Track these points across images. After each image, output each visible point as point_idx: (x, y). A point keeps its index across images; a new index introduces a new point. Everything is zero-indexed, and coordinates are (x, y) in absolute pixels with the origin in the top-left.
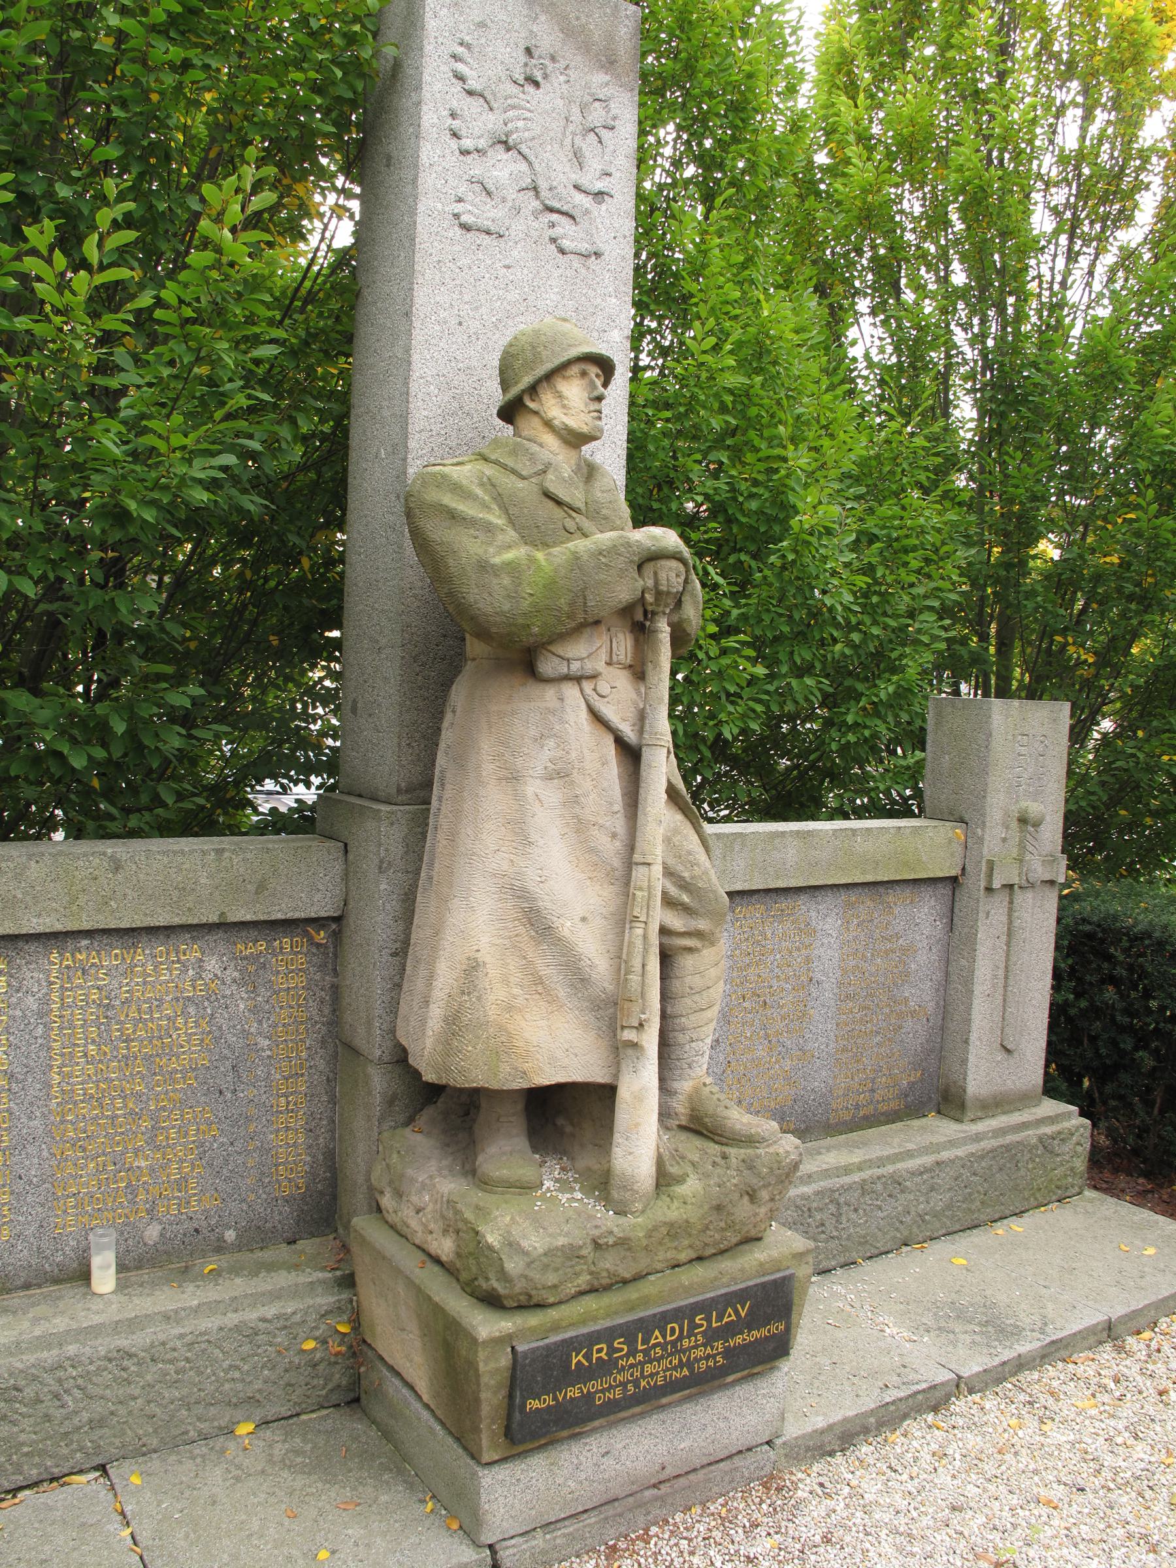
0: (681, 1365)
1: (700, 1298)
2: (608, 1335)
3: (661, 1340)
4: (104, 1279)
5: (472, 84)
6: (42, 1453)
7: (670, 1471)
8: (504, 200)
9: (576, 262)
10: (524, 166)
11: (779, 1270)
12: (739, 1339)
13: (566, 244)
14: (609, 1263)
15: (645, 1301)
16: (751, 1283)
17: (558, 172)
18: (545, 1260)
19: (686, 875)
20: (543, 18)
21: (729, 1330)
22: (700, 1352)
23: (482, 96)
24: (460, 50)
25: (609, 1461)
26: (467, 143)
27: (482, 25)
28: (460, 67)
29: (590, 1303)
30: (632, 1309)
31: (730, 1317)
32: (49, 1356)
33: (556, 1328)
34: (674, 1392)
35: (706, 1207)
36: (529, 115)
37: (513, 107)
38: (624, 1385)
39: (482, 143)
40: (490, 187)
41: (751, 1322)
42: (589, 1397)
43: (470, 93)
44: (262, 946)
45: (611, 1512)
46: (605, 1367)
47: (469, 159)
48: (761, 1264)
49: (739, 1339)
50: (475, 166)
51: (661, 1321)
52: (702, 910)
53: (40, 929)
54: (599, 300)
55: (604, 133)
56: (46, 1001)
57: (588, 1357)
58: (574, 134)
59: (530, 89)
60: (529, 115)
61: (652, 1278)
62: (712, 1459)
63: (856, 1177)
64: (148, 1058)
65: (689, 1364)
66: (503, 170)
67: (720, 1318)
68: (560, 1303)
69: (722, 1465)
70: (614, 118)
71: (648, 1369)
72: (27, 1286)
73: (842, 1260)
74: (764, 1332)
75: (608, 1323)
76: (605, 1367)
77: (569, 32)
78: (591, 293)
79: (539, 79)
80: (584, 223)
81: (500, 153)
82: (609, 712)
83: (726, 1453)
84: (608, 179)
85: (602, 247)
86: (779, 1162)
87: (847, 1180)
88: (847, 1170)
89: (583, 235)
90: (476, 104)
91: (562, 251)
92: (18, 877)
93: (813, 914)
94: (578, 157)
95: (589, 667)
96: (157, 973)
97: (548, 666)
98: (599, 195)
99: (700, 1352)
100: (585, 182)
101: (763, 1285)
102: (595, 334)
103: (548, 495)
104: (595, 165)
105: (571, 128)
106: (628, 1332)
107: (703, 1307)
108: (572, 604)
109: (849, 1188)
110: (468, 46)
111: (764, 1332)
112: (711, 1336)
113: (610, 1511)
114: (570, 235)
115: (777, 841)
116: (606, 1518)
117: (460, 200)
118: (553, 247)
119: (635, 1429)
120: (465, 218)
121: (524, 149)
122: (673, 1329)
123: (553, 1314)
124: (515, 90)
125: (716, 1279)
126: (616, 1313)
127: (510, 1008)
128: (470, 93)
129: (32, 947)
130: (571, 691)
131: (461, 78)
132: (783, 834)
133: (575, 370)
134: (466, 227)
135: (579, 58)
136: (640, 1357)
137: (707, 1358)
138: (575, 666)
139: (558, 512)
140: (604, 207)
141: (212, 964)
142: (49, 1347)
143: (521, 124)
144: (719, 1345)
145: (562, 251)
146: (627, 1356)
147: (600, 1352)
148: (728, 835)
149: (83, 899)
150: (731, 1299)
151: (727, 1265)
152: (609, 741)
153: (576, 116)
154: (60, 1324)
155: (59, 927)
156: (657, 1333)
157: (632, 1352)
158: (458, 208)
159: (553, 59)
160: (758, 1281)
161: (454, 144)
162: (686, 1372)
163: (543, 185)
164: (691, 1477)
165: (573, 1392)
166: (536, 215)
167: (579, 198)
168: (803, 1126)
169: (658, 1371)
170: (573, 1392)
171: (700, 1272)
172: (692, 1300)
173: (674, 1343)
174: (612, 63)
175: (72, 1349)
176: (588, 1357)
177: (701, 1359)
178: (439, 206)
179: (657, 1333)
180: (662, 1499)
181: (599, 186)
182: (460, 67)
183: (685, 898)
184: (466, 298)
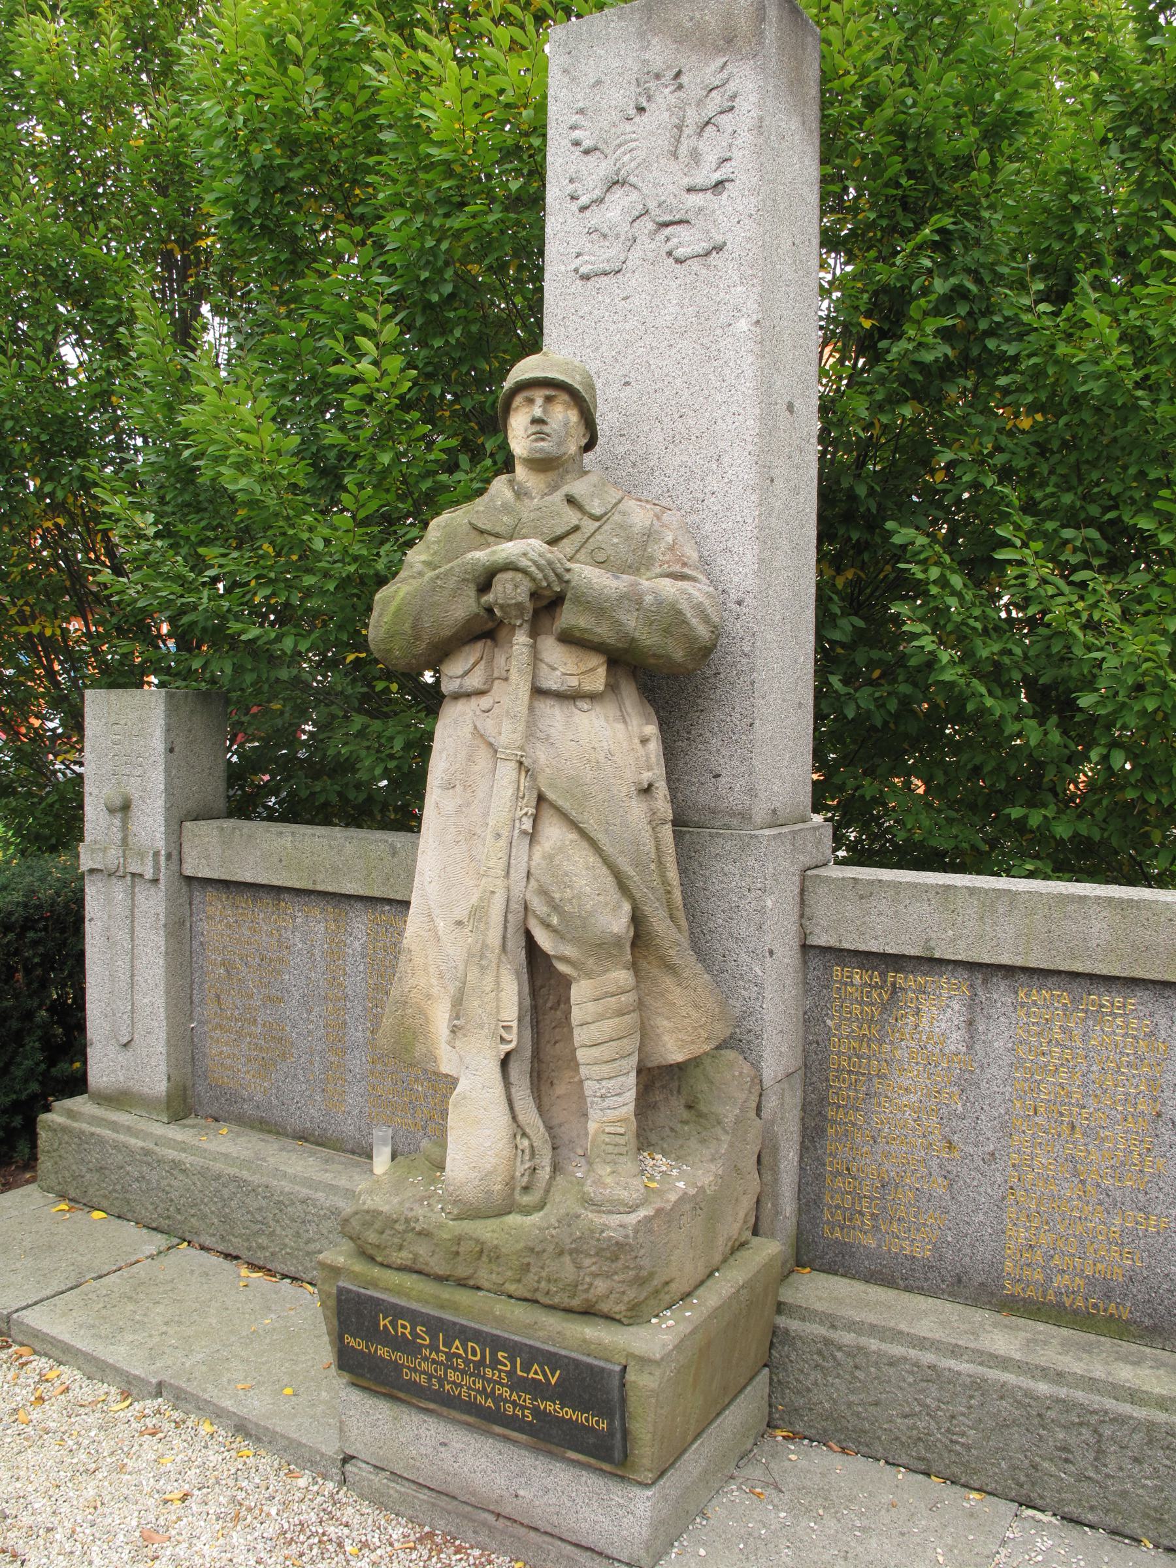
1: (506, 1335)
2: (414, 1317)
3: (461, 1352)
4: (381, 1162)
5: (587, 143)
6: (297, 1257)
7: (507, 1510)
8: (618, 236)
9: (695, 265)
11: (607, 1360)
12: (549, 1407)
13: (680, 252)
14: (422, 1249)
15: (455, 1307)
16: (564, 1352)
18: (368, 1217)
19: (557, 896)
20: (655, 41)
21: (537, 1389)
23: (596, 149)
24: (576, 118)
25: (445, 1454)
26: (584, 200)
27: (598, 83)
28: (577, 134)
29: (409, 1281)
30: (442, 1307)
31: (535, 1373)
32: (304, 1192)
33: (374, 1284)
34: (469, 1413)
35: (522, 1245)
36: (633, 145)
37: (619, 146)
38: (430, 1376)
39: (597, 193)
40: (605, 230)
41: (562, 1394)
42: (398, 1367)
43: (587, 152)
45: (442, 1504)
46: (408, 1346)
47: (588, 213)
48: (585, 1341)
49: (549, 1407)
50: (594, 217)
51: (466, 1334)
52: (569, 936)
53: (352, 892)
54: (722, 295)
57: (394, 1324)
58: (689, 137)
60: (633, 145)
61: (481, 1293)
62: (556, 1531)
63: (1140, 1413)
65: (498, 1399)
66: (618, 207)
67: (527, 1368)
68: (388, 1267)
69: (563, 1545)
70: (733, 97)
71: (452, 1376)
72: (353, 1152)
73: (1113, 1521)
74: (581, 1418)
75: (414, 1305)
76: (408, 1346)
77: (682, 38)
78: (713, 291)
79: (645, 104)
80: (699, 223)
81: (618, 192)
83: (574, 1539)
84: (728, 164)
85: (719, 239)
86: (592, 1232)
87: (1126, 1408)
88: (1134, 1396)
89: (700, 236)
90: (591, 159)
91: (679, 261)
92: (339, 852)
93: (1163, 1023)
94: (695, 155)
98: (719, 185)
101: (577, 1363)
102: (719, 332)
104: (711, 157)
105: (687, 131)
106: (435, 1326)
107: (514, 1350)
108: (414, 627)
109: (1120, 1420)
110: (581, 111)
111: (581, 1418)
112: (519, 1385)
113: (443, 1502)
114: (687, 240)
115: (1071, 908)
116: (434, 1505)
117: (578, 255)
118: (671, 260)
119: (489, 1446)
120: (582, 270)
121: (632, 179)
122: (474, 1353)
123: (376, 1271)
124: (628, 127)
125: (529, 1326)
126: (427, 1302)
127: (429, 996)
128: (587, 152)
129: (359, 905)
131: (577, 143)
132: (1083, 899)
134: (586, 278)
135: (694, 57)
136: (442, 1358)
137: (514, 1403)
140: (725, 195)
142: (310, 1187)
143: (626, 158)
145: (679, 261)
147: (404, 1328)
148: (986, 891)
149: (374, 875)
150: (551, 1360)
151: (552, 1323)
154: (328, 1177)
156: (457, 1342)
157: (434, 1347)
159: (658, 77)
160: (574, 1355)
161: (574, 207)
162: (490, 1403)
163: (652, 205)
164: (532, 1534)
165: (383, 1352)
168: (1148, 1322)
169: (465, 1386)
170: (383, 1352)
171: (520, 1313)
172: (498, 1332)
174: (730, 41)
175: (320, 1195)
177: (506, 1401)
178: (563, 268)
179: (457, 1342)
180: (491, 1528)
181: (717, 176)
182: (577, 134)
183: (555, 920)
184: (588, 342)
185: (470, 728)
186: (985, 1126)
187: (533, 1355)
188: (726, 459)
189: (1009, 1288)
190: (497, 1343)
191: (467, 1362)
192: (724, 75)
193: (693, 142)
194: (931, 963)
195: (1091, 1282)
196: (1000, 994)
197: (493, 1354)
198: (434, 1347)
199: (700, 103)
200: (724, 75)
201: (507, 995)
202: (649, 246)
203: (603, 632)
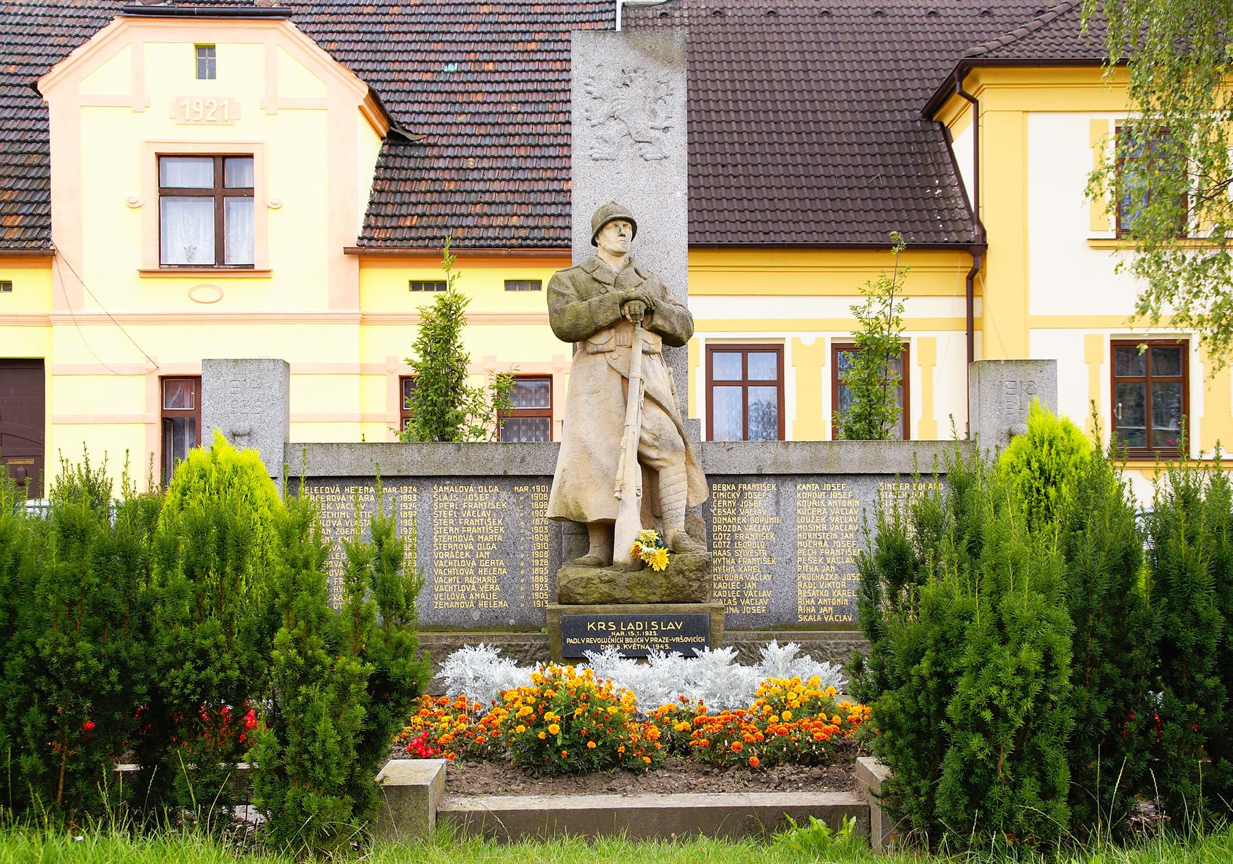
0: (645, 643)
5: (595, 94)
10: (623, 125)
12: (678, 639)
13: (647, 156)
17: (641, 123)
22: (656, 640)
26: (594, 122)
28: (589, 88)
31: (671, 626)
39: (601, 120)
44: (526, 488)
49: (678, 639)
50: (600, 132)
55: (668, 98)
56: (431, 506)
57: (596, 626)
59: (624, 89)
64: (474, 534)
66: (613, 129)
71: (627, 640)
80: (657, 144)
81: (613, 122)
82: (617, 365)
85: (667, 154)
93: (857, 492)
94: (654, 113)
95: (606, 348)
96: (480, 499)
97: (590, 349)
99: (656, 640)
100: (656, 124)
103: (595, 280)
104: (662, 115)
130: (600, 357)
133: (610, 225)
138: (600, 348)
139: (596, 285)
141: (504, 495)
144: (666, 639)
146: (616, 631)
152: (619, 377)
153: (651, 93)
155: (435, 474)
157: (618, 630)
158: (591, 152)
163: (633, 132)
166: (631, 145)
167: (653, 133)
173: (641, 632)
176: (596, 626)
181: (665, 124)
185: (606, 367)
186: (786, 547)
187: (668, 619)
188: (672, 253)
189: (802, 619)
190: (650, 619)
191: (635, 632)
192: (669, 78)
193: (653, 105)
194: (760, 476)
195: (835, 607)
196: (788, 487)
197: (649, 624)
198: (618, 630)
199: (656, 88)
200: (669, 78)
201: (633, 476)
202: (629, 150)
203: (668, 328)
